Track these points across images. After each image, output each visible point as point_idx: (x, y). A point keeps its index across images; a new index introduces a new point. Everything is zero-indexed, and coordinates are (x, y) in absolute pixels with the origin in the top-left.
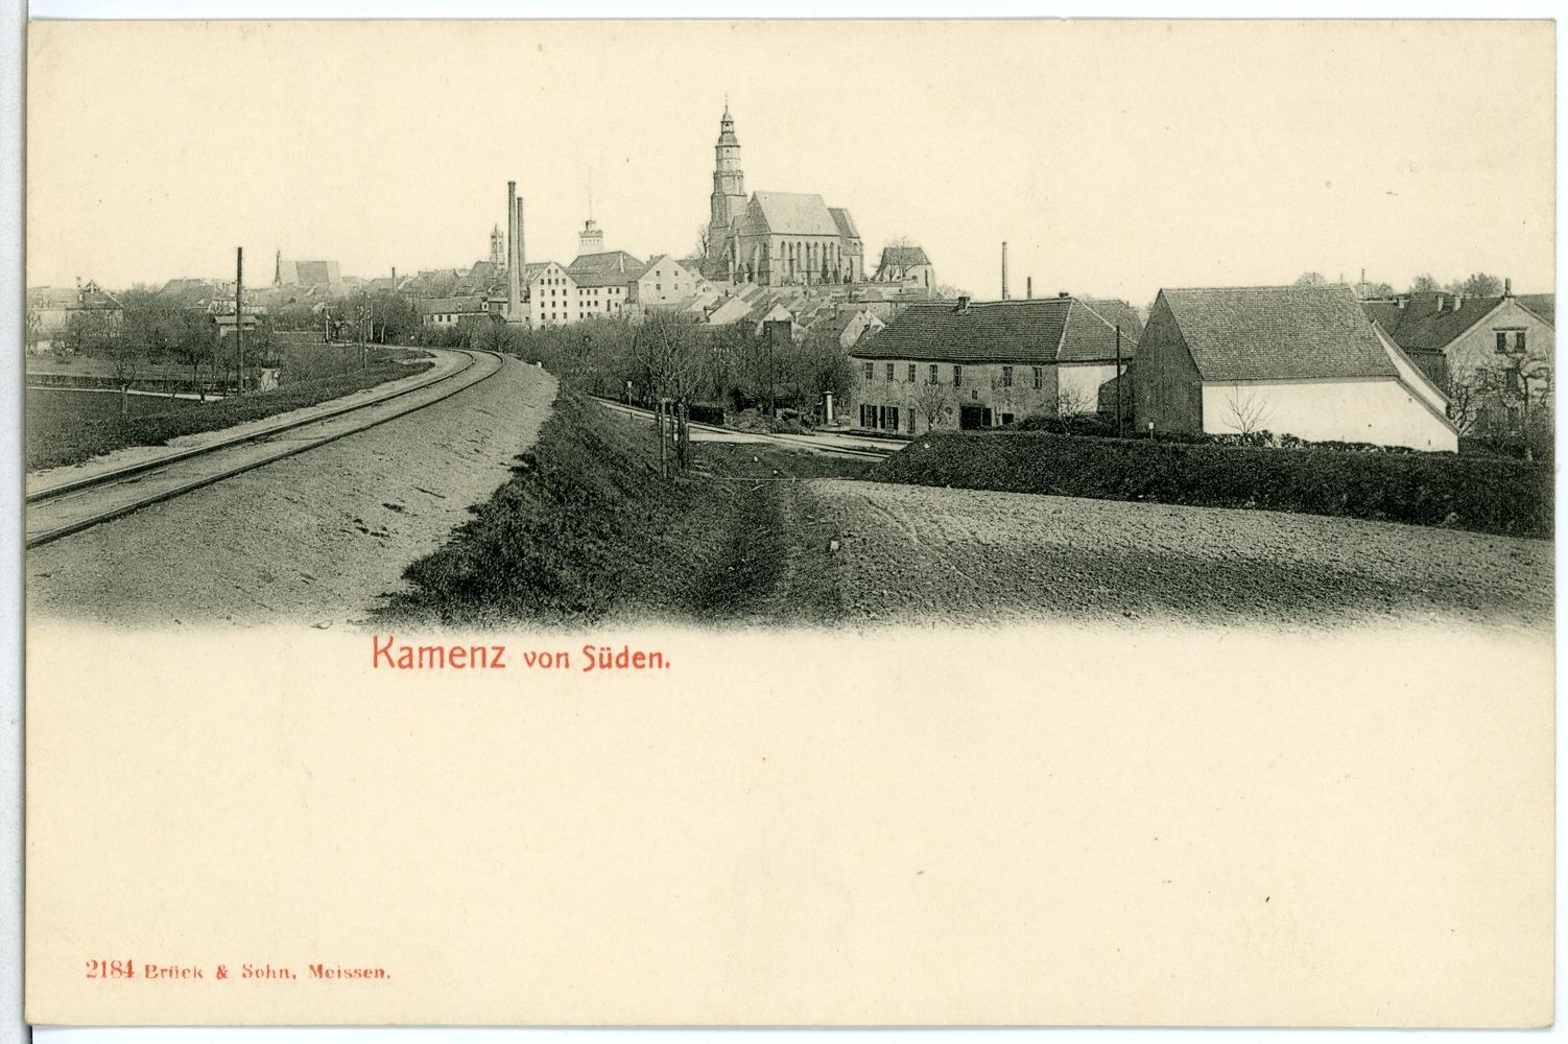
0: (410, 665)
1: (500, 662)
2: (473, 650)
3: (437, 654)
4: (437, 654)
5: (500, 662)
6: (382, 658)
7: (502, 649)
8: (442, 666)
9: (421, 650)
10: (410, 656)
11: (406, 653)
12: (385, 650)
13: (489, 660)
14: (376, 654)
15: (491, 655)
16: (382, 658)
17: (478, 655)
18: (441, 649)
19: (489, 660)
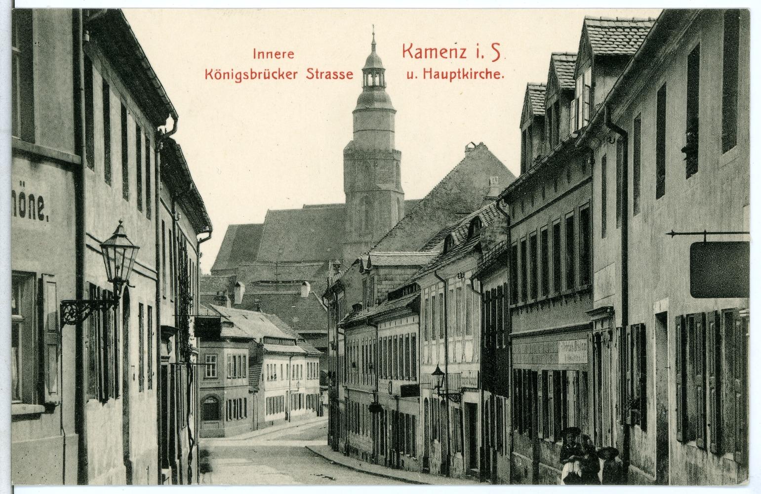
0: (421, 57)
1: (463, 56)
2: (451, 50)
3: (434, 52)
4: (434, 52)
5: (463, 56)
6: (407, 53)
7: (465, 50)
8: (436, 57)
9: (426, 50)
10: (421, 53)
11: (419, 51)
12: (408, 50)
13: (459, 55)
14: (404, 51)
15: (460, 52)
16: (407, 53)
17: (453, 52)
18: (436, 49)
19: (459, 55)
